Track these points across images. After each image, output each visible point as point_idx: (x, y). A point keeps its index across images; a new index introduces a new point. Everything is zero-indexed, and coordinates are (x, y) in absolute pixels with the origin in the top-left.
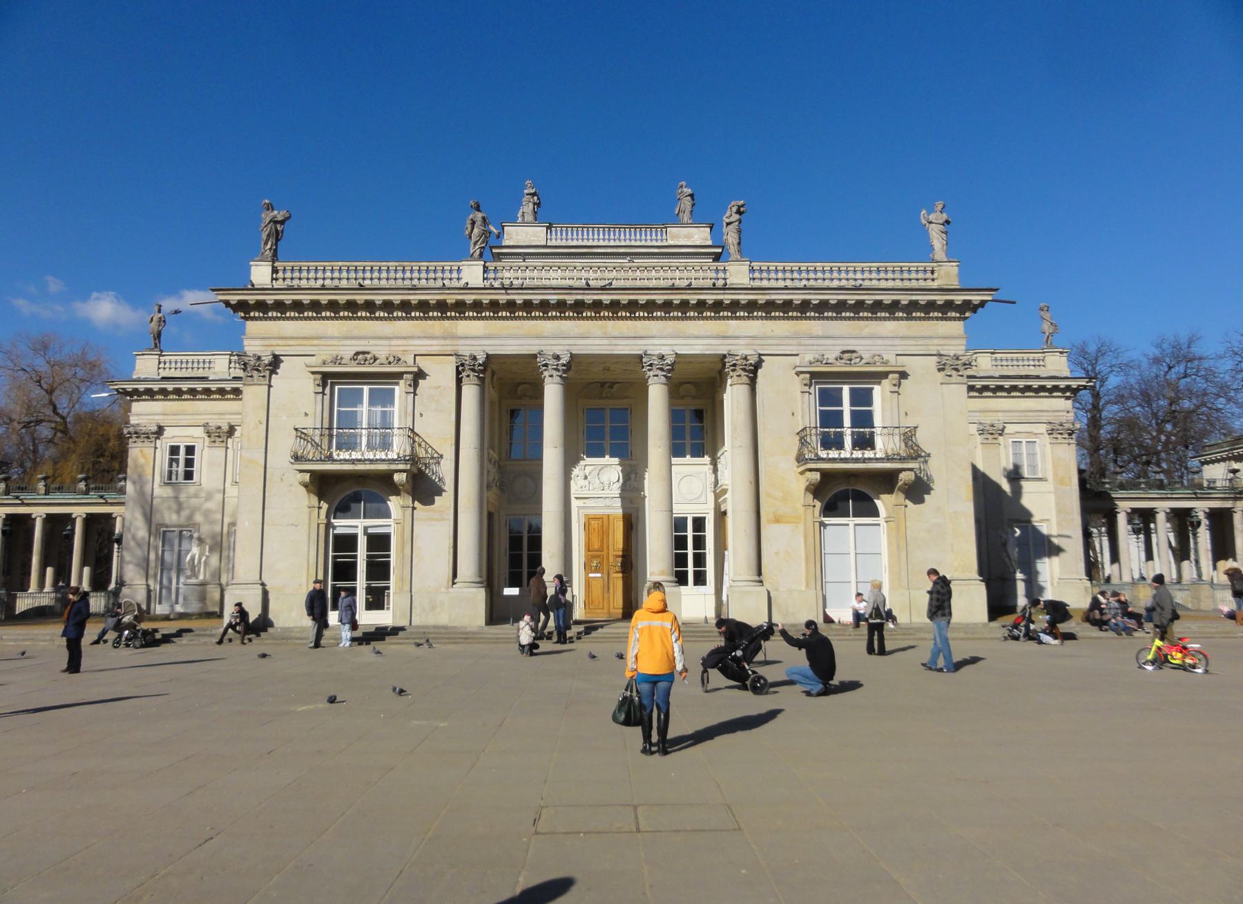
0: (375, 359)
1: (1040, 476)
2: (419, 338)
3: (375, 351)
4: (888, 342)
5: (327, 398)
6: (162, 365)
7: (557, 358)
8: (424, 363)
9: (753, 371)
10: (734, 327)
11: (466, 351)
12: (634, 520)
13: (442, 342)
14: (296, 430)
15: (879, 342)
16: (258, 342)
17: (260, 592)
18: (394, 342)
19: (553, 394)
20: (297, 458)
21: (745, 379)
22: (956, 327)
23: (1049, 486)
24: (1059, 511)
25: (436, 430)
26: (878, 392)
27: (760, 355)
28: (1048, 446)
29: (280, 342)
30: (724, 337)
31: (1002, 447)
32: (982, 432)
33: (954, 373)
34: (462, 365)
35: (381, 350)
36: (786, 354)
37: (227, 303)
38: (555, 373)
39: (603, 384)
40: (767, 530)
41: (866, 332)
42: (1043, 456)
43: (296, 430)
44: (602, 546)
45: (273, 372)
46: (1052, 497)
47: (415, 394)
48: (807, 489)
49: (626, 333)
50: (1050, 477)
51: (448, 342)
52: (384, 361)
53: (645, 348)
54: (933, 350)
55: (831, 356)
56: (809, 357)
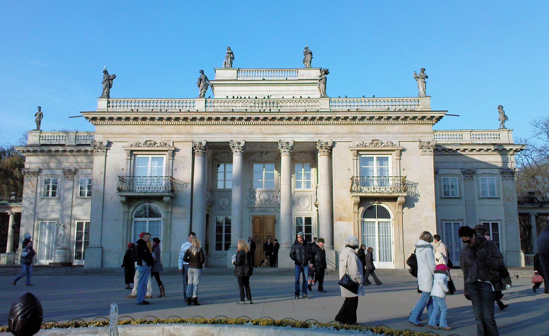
0: (155, 143)
1: (496, 196)
2: (175, 134)
3: (155, 140)
4: (395, 136)
5: (132, 161)
6: (41, 138)
7: (239, 143)
8: (177, 146)
9: (330, 150)
11: (197, 140)
12: (277, 219)
13: (186, 136)
14: (119, 177)
15: (391, 136)
16: (101, 136)
17: (100, 251)
18: (163, 136)
20: (119, 190)
21: (326, 153)
22: (428, 128)
23: (501, 202)
24: (506, 215)
25: (183, 175)
26: (390, 157)
27: (334, 142)
28: (501, 181)
29: (111, 136)
30: (317, 134)
31: (475, 181)
32: (464, 173)
33: (427, 150)
34: (195, 147)
35: (158, 139)
36: (346, 140)
37: (87, 118)
38: (238, 150)
39: (262, 153)
40: (336, 224)
41: (385, 130)
42: (498, 186)
43: (119, 177)
44: (261, 231)
45: (107, 149)
46: (502, 208)
47: (173, 160)
48: (355, 204)
49: (270, 131)
50: (501, 196)
51: (188, 136)
52: (159, 145)
53: (280, 139)
54: (417, 139)
55: (368, 142)
56: (357, 143)
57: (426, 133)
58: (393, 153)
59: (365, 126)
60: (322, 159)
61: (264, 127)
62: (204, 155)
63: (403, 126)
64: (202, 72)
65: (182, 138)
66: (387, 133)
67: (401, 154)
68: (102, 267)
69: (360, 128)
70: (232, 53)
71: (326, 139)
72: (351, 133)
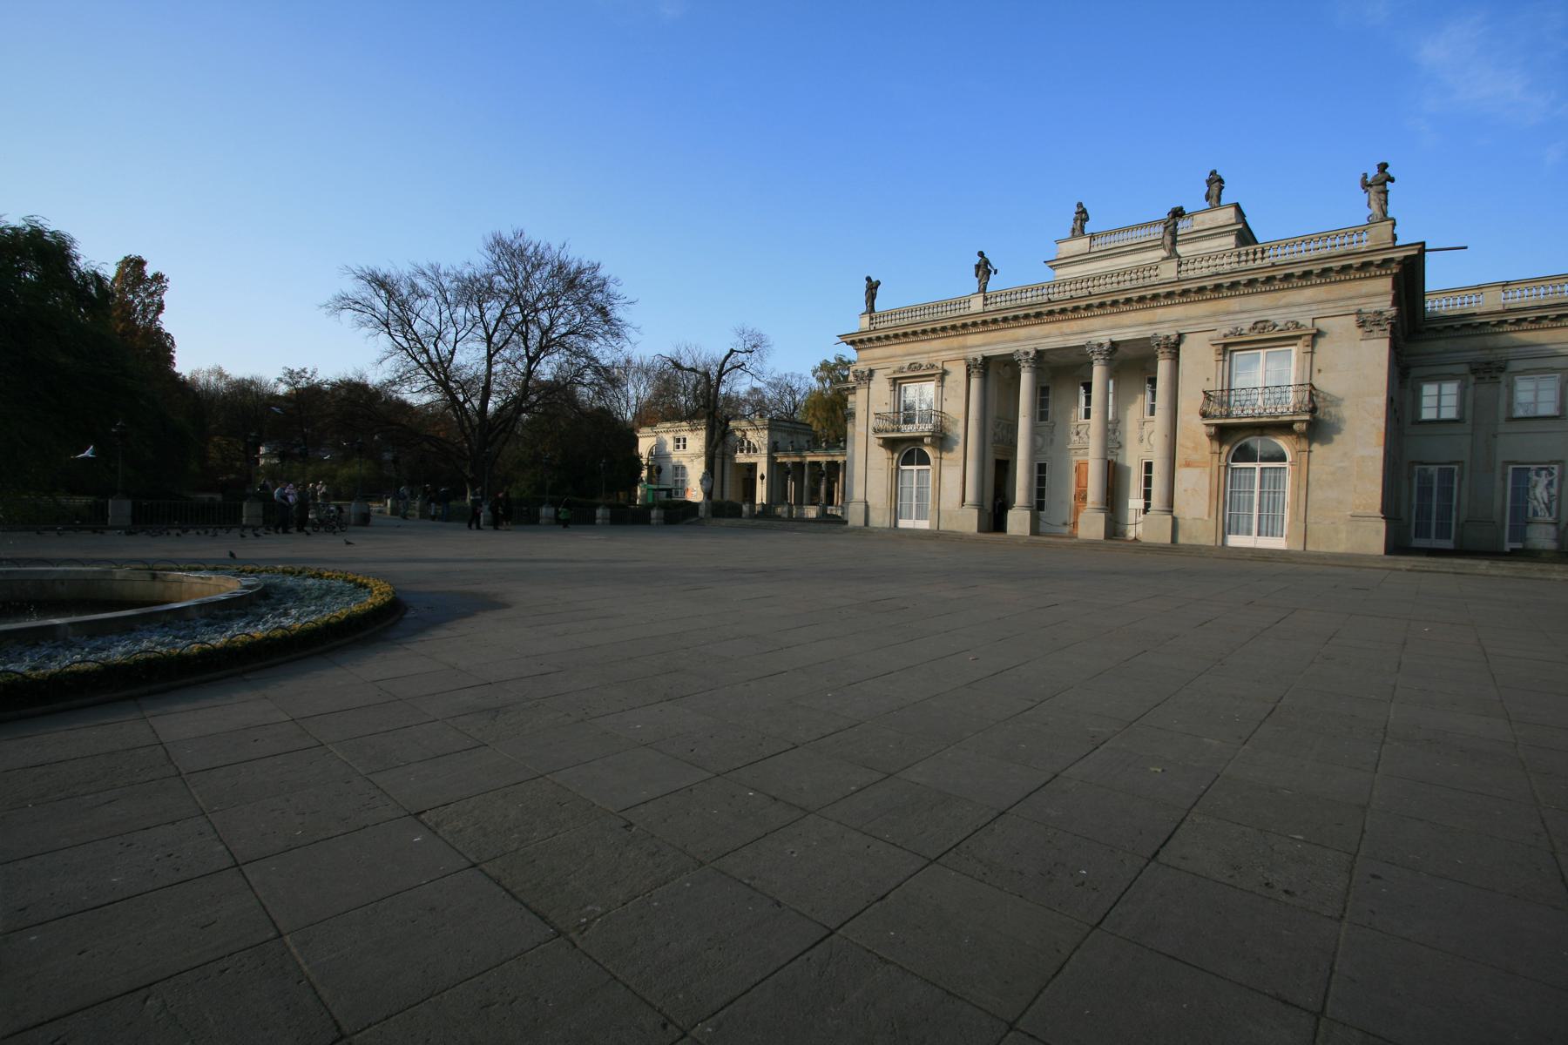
7: (1027, 353)
9: (1174, 347)
10: (1160, 313)
19: (1026, 379)
25: (954, 408)
27: (1180, 336)
40: (1180, 473)
54: (1353, 309)
55: (1246, 327)
57: (1376, 295)
58: (1300, 342)
59: (1243, 299)
60: (1163, 367)
61: (1065, 324)
62: (984, 376)
63: (1323, 288)
64: (981, 254)
65: (953, 354)
66: (1286, 306)
67: (1313, 344)
68: (866, 523)
69: (1234, 304)
70: (1084, 211)
71: (1169, 331)
72: (1214, 314)
